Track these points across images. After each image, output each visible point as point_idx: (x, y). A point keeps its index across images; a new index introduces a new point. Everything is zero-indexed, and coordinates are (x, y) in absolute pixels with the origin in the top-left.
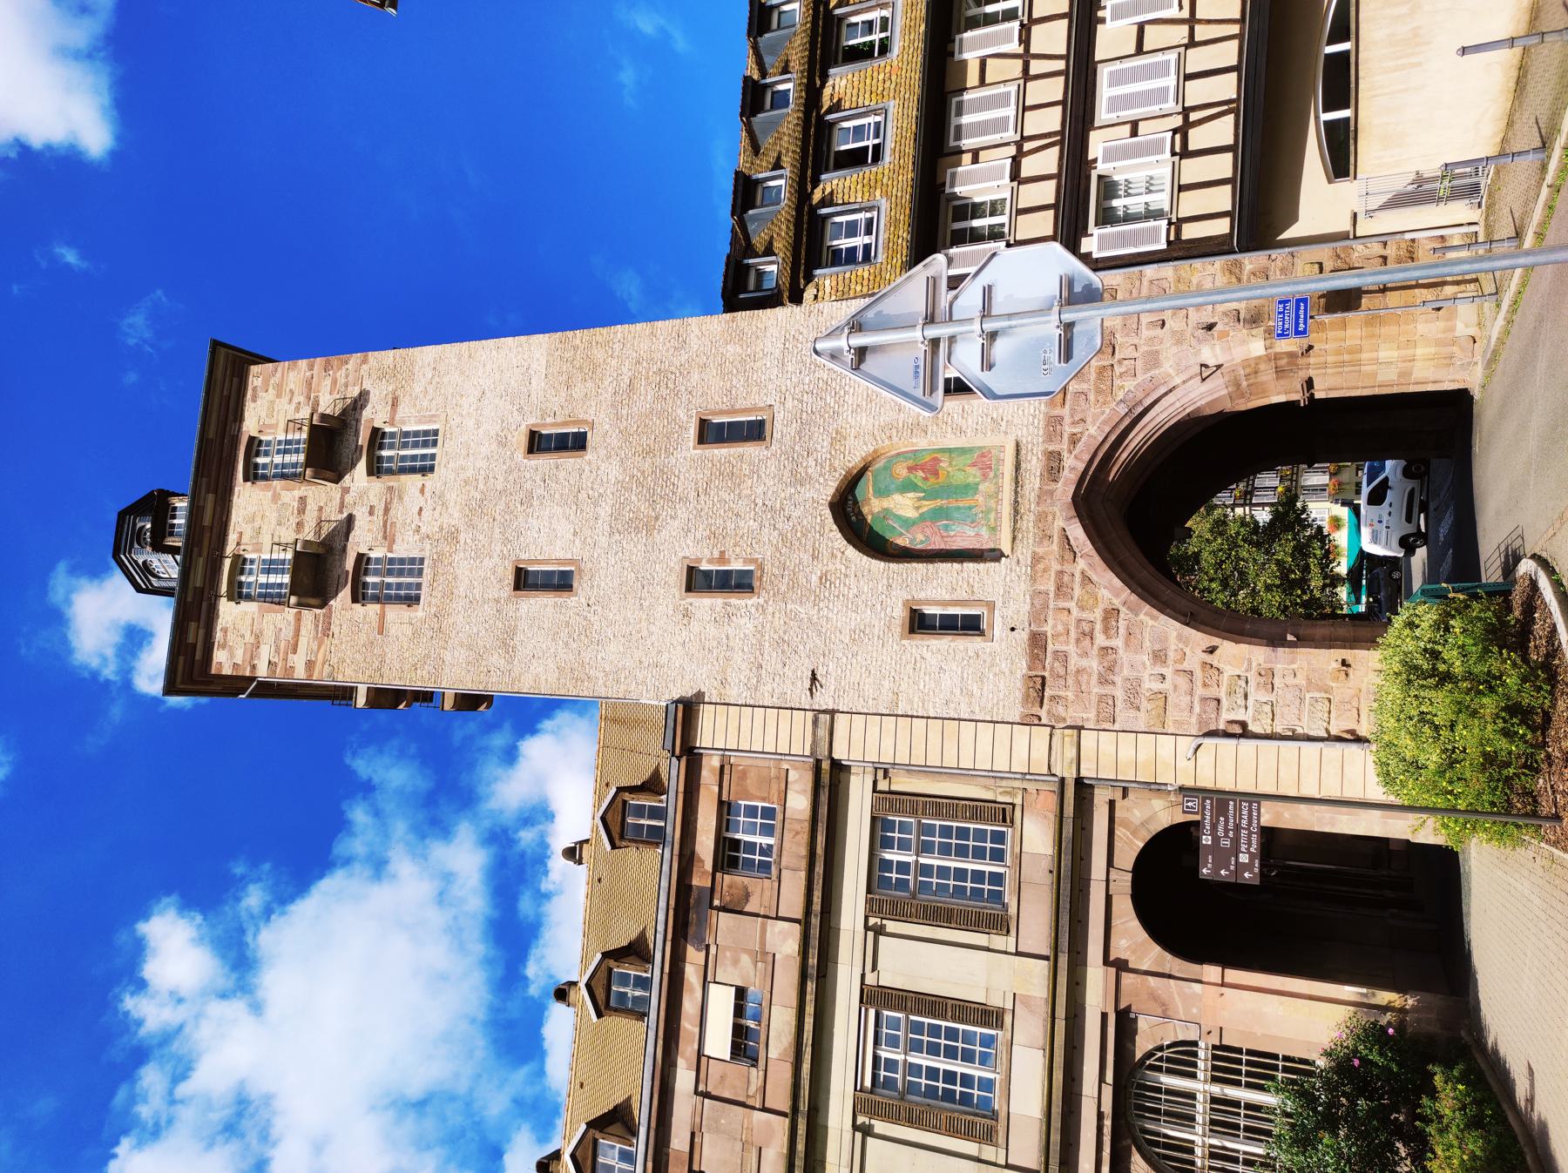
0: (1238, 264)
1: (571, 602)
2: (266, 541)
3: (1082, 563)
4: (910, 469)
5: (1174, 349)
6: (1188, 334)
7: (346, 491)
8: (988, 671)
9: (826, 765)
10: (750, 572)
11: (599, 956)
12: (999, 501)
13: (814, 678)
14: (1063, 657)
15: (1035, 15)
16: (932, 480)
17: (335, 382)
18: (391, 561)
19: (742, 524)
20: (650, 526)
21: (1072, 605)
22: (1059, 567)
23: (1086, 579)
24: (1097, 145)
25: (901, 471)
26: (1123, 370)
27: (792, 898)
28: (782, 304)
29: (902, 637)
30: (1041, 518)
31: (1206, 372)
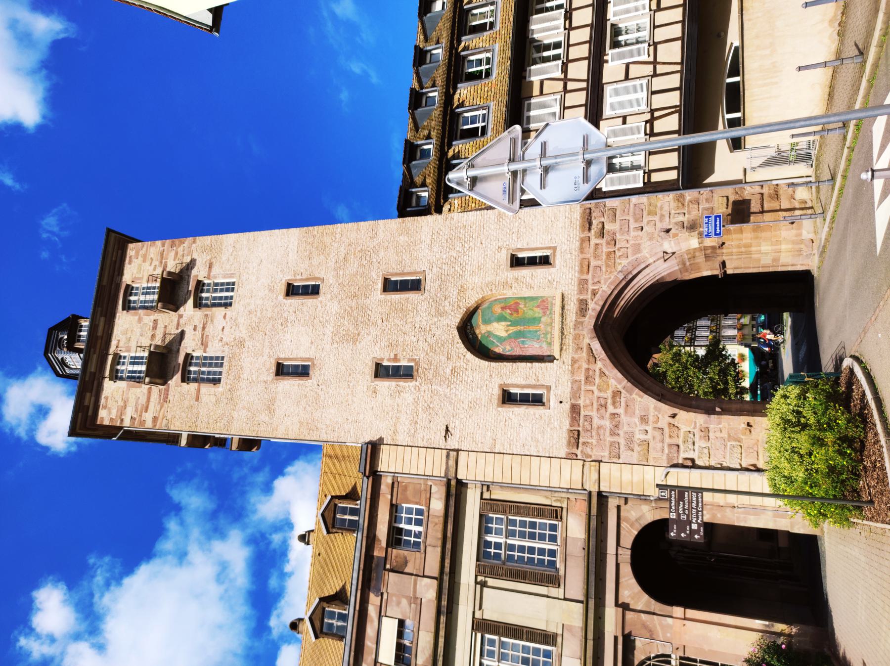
0: (682, 196)
2: (133, 345)
3: (599, 364)
5: (649, 243)
6: (656, 235)
7: (181, 316)
8: (546, 427)
9: (453, 483)
10: (412, 367)
11: (317, 600)
13: (447, 430)
14: (589, 419)
15: (570, 58)
16: (515, 315)
17: (177, 253)
18: (205, 358)
19: (407, 338)
20: (355, 339)
22: (587, 366)
23: (602, 373)
25: (498, 309)
26: (620, 253)
27: (433, 567)
28: (431, 214)
29: (498, 406)
30: (576, 337)
31: (666, 256)
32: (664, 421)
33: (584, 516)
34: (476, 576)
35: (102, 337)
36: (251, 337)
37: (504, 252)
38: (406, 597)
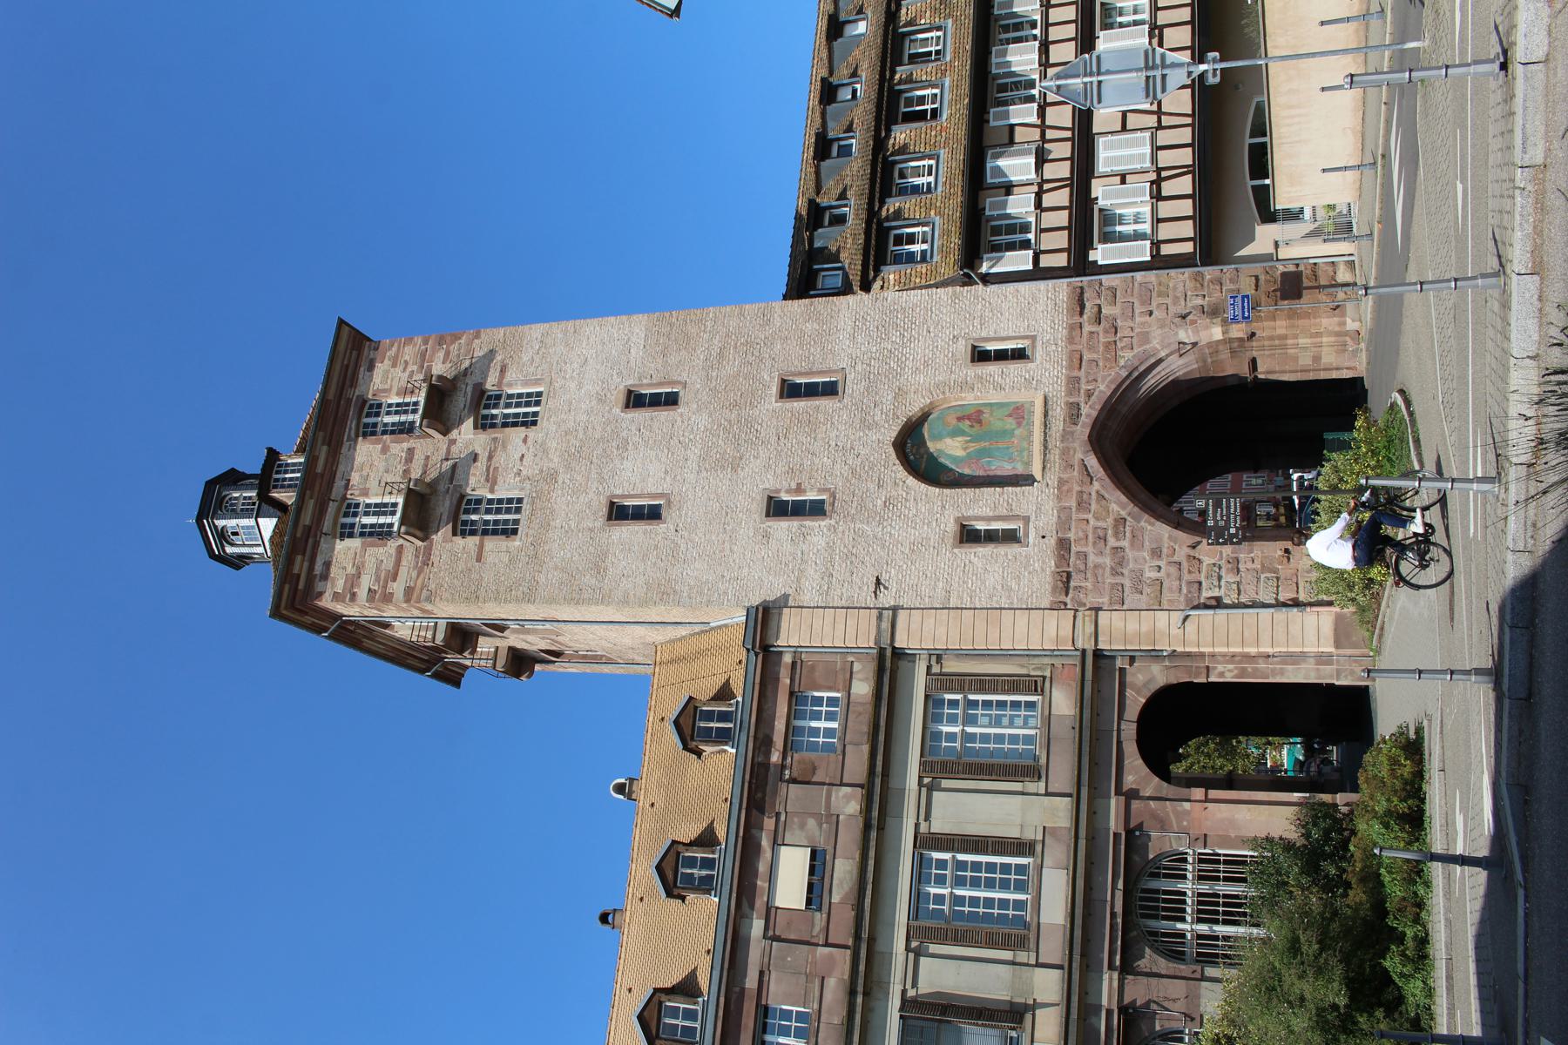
1: (658, 528)
4: (959, 419)
7: (453, 442)
10: (822, 502)
12: (1030, 443)
13: (878, 582)
14: (1084, 556)
17: (447, 353)
21: (1090, 517)
23: (1101, 497)
24: (1098, 189)
29: (954, 546)
30: (1065, 452)
31: (1181, 349)
32: (1182, 553)
33: (1075, 685)
34: (920, 778)
35: (322, 475)
36: (568, 468)
37: (962, 342)
38: (813, 815)
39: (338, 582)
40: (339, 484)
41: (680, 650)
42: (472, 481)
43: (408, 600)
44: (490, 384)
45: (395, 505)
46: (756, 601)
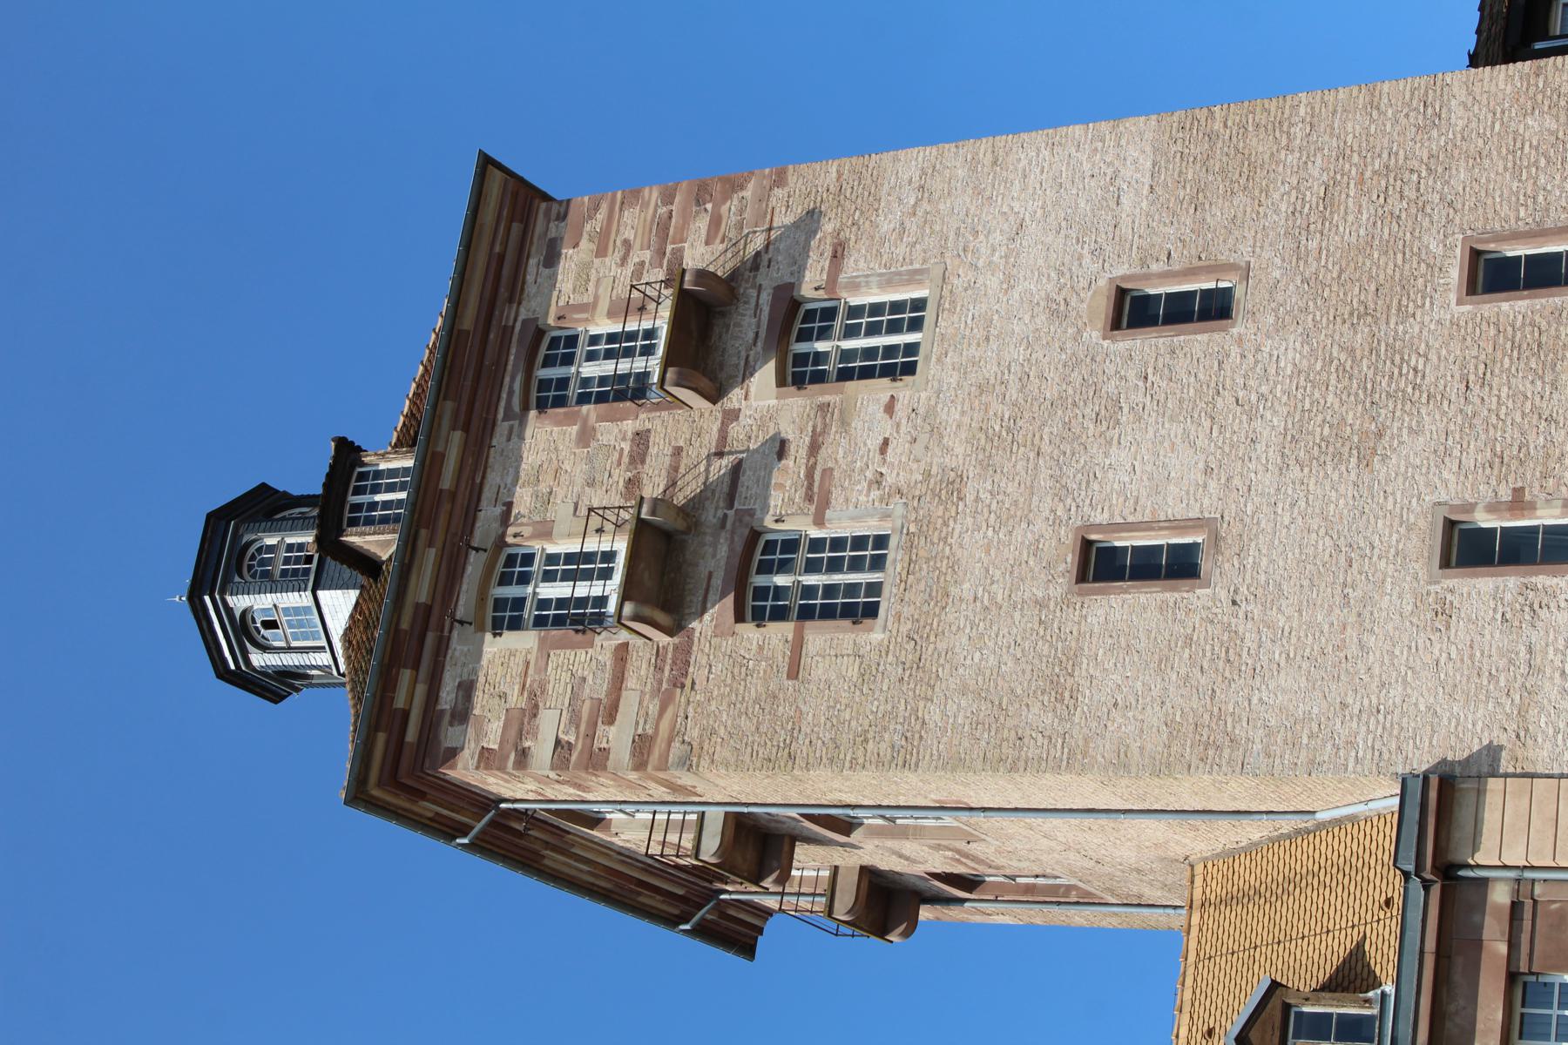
7: (732, 416)
17: (716, 222)
35: (453, 495)
36: (987, 465)
39: (490, 724)
40: (489, 513)
41: (1247, 875)
42: (776, 500)
43: (640, 765)
44: (810, 286)
45: (609, 556)
46: (1422, 762)
